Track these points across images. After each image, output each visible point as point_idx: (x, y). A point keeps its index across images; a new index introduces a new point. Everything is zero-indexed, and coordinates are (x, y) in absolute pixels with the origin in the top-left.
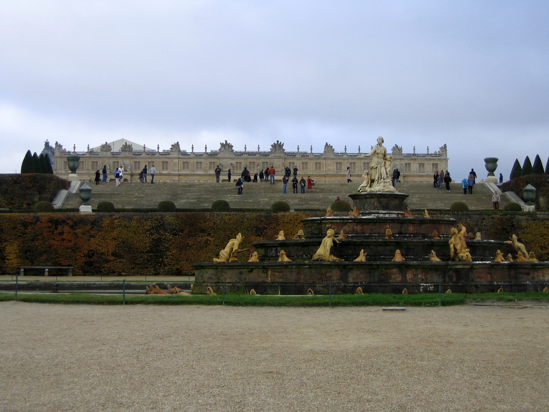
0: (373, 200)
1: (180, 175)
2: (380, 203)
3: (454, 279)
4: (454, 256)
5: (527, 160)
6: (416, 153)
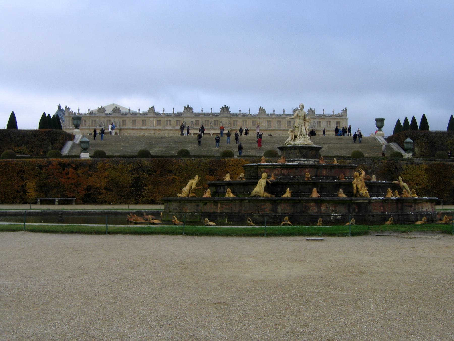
0: (296, 151)
1: (155, 130)
2: (301, 153)
3: (357, 211)
4: (357, 193)
5: (406, 120)
6: (325, 114)
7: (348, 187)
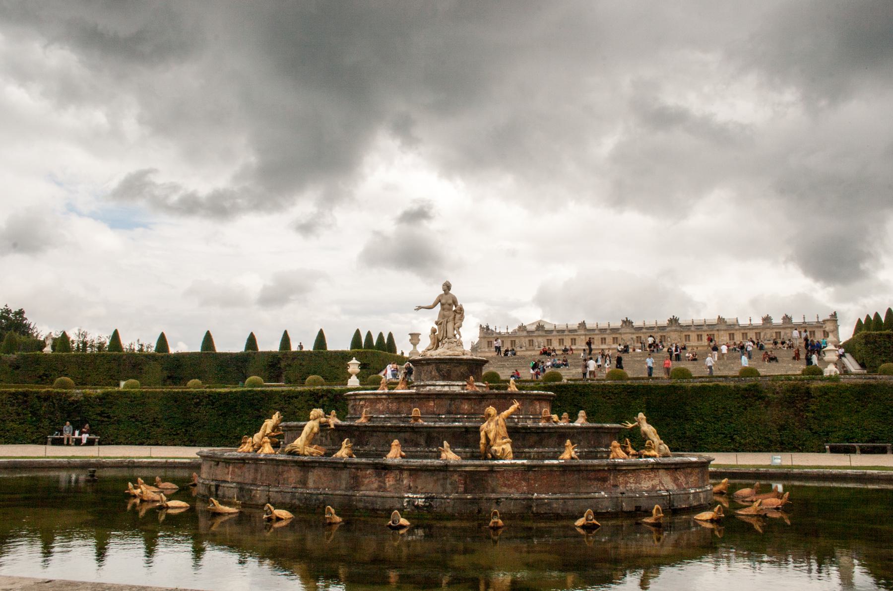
3: (461, 489)
5: (868, 316)
7: (467, 438)
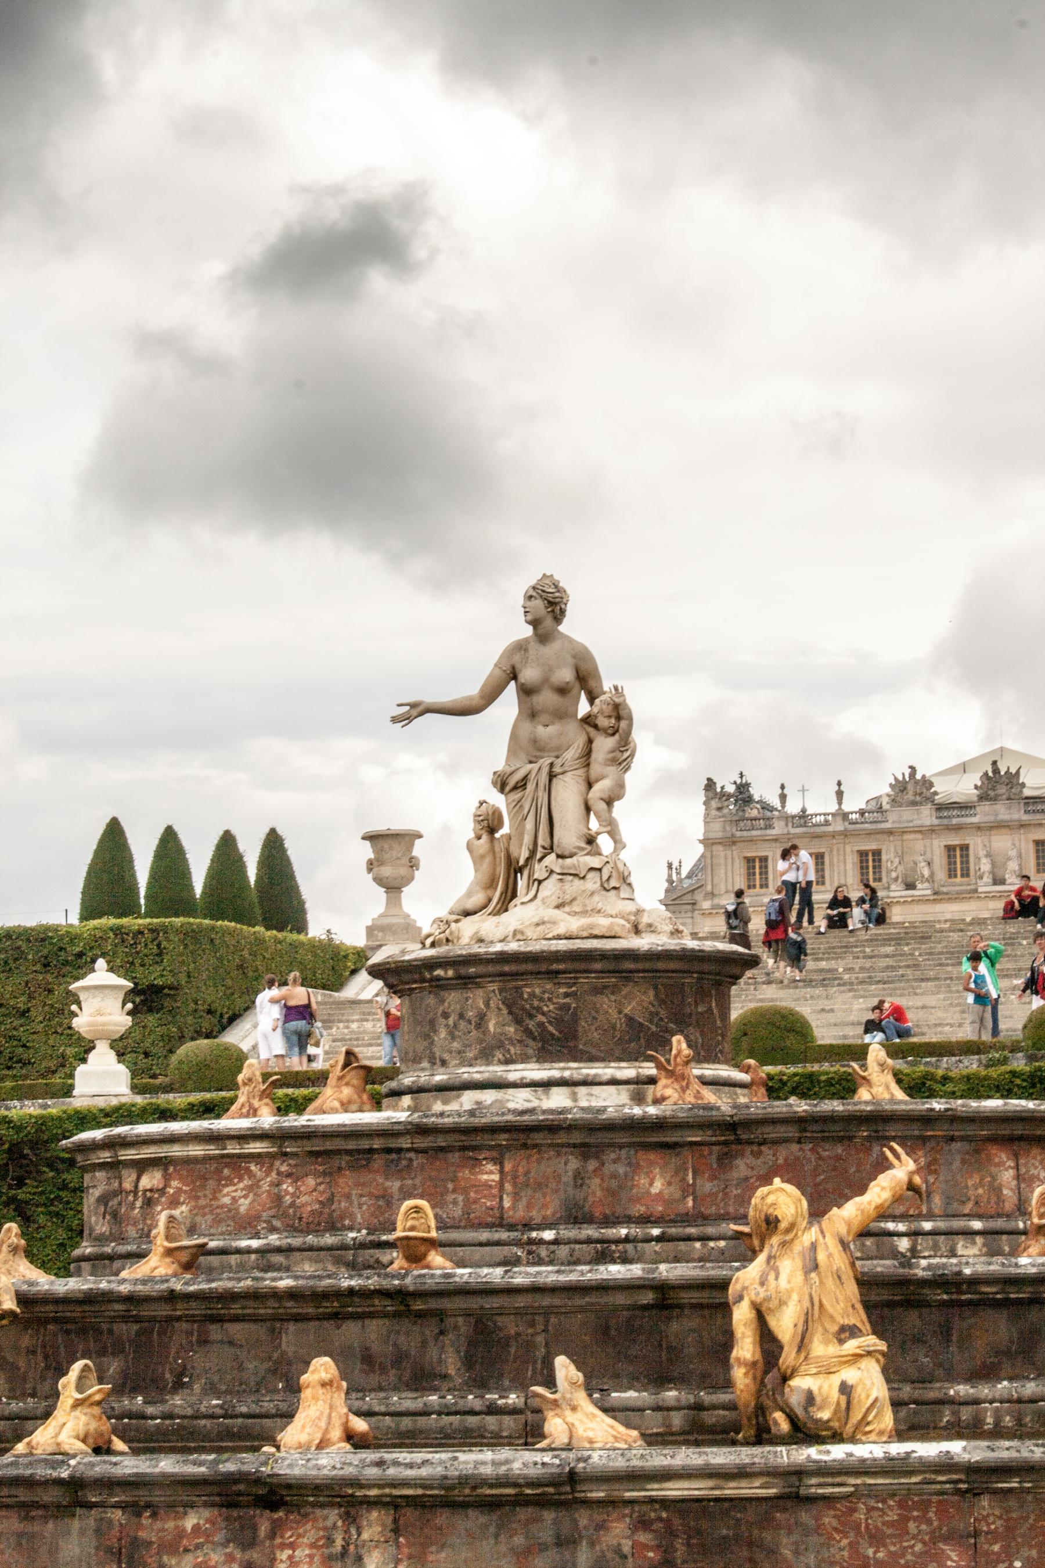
0: (476, 999)
2: (518, 1012)
7: (662, 1339)
